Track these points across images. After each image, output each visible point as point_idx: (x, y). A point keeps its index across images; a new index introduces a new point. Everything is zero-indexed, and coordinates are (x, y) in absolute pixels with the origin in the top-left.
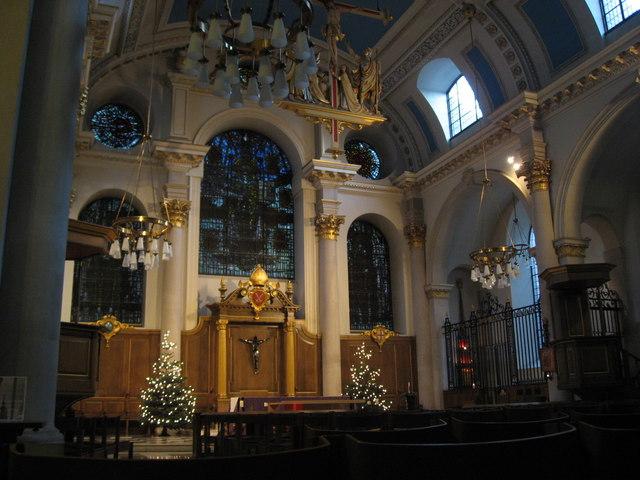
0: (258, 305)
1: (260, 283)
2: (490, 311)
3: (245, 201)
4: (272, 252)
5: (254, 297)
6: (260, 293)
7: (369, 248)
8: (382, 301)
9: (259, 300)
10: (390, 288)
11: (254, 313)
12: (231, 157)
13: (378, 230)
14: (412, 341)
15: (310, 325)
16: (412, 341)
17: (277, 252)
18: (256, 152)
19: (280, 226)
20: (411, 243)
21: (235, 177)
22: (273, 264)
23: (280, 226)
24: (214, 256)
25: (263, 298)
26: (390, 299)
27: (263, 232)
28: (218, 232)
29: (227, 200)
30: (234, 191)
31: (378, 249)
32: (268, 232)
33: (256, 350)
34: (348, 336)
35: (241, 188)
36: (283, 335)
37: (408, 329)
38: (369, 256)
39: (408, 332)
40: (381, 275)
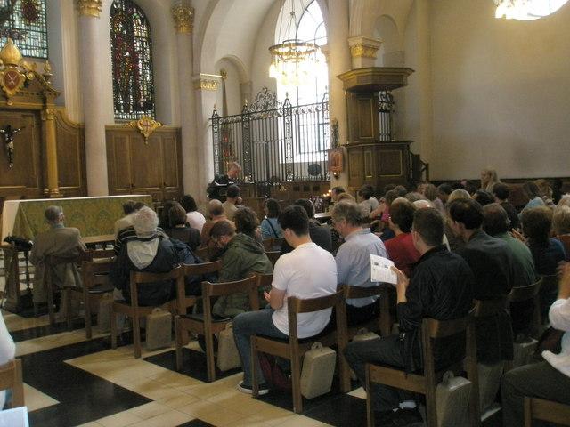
0: (11, 87)
1: (13, 62)
2: (265, 107)
4: (19, 23)
7: (129, 26)
8: (143, 89)
9: (12, 82)
10: (151, 75)
11: (6, 98)
13: (139, 8)
14: (178, 133)
15: (72, 115)
16: (178, 133)
17: (26, 25)
20: (177, 28)
22: (22, 39)
25: (17, 80)
26: (152, 90)
31: (140, 31)
33: (10, 141)
34: (113, 127)
36: (40, 125)
37: (173, 118)
38: (131, 39)
39: (173, 123)
40: (143, 60)
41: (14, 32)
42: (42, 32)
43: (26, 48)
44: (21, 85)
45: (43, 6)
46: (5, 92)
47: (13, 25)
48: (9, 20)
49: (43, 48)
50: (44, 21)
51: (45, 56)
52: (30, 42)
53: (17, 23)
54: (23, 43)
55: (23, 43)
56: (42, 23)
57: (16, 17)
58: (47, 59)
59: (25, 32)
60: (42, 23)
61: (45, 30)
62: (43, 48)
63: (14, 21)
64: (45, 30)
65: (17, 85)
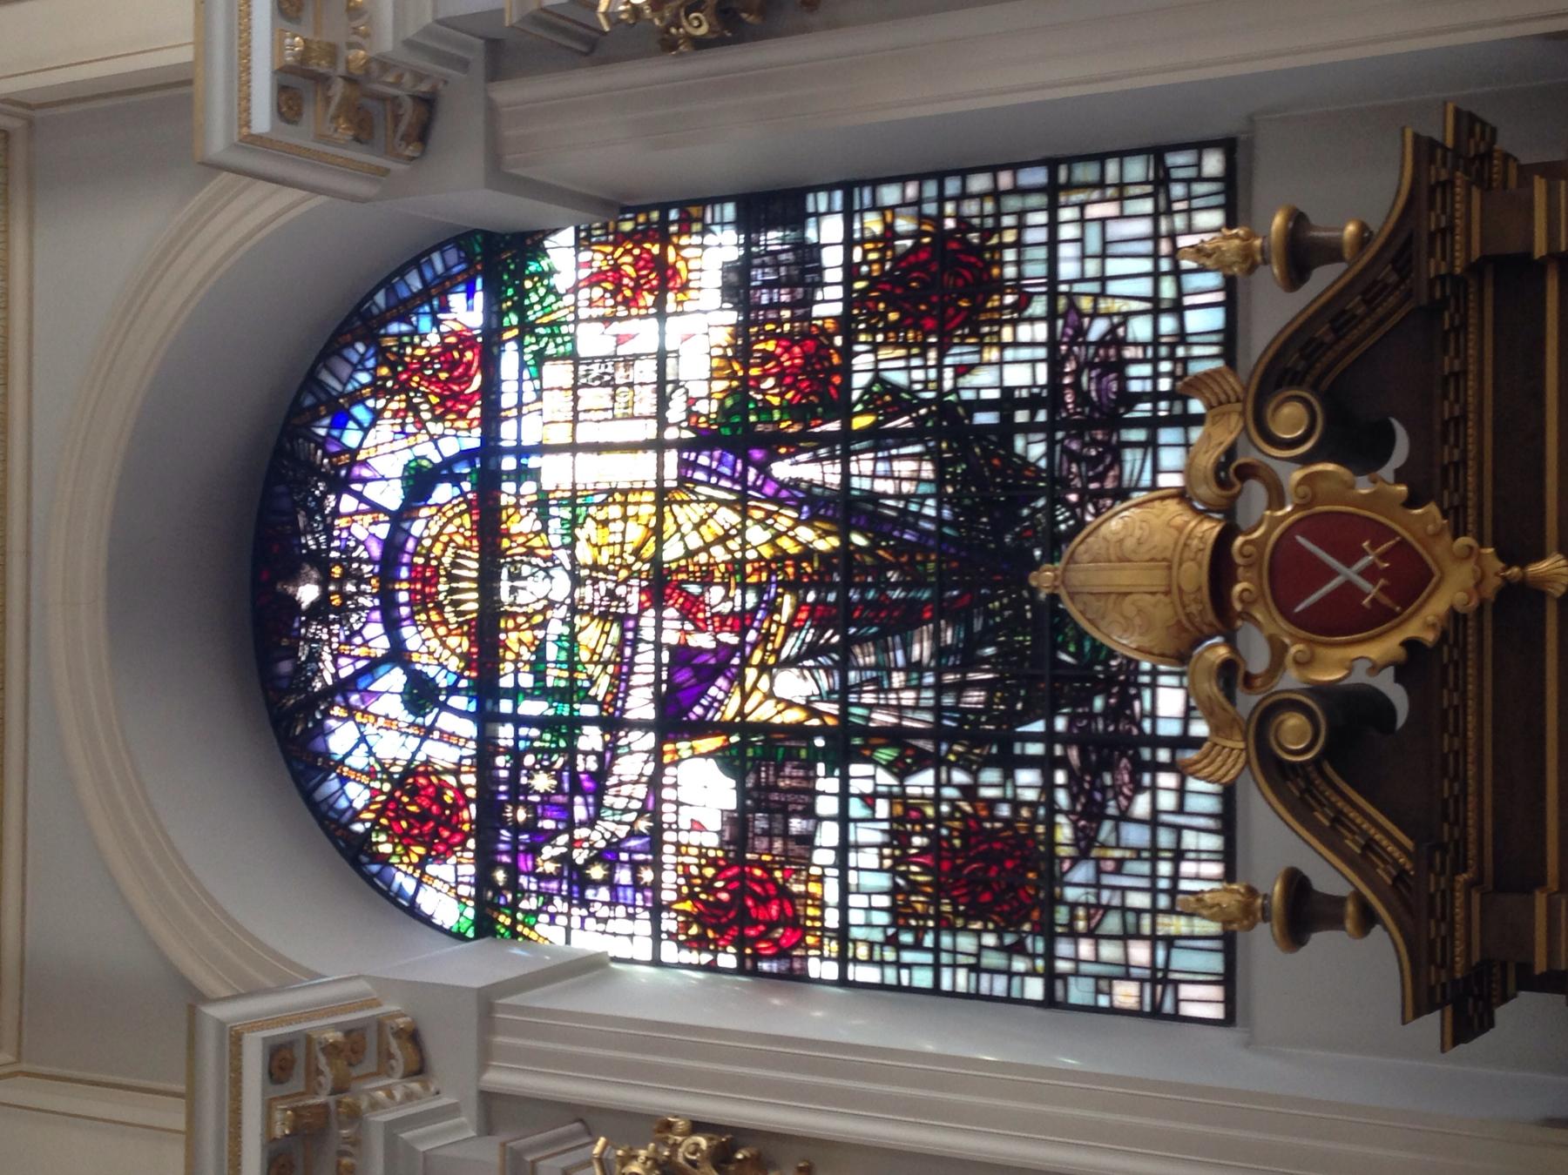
0: (1409, 578)
3: (661, 585)
4: (1015, 365)
5: (1343, 619)
6: (1288, 572)
11: (1516, 606)
12: (421, 695)
18: (375, 508)
19: (828, 305)
21: (538, 667)
23: (828, 305)
24: (1085, 844)
25: (1344, 532)
27: (879, 440)
28: (906, 815)
29: (676, 719)
30: (623, 674)
32: (886, 398)
35: (603, 616)
41: (1082, 397)
42: (1053, 193)
43: (1178, 308)
44: (1374, 489)
45: (890, 195)
46: (1455, 616)
47: (1033, 403)
48: (1007, 429)
49: (1161, 182)
50: (979, 183)
51: (1213, 163)
52: (1130, 278)
53: (1017, 376)
54: (1140, 329)
55: (1140, 329)
56: (996, 194)
57: (984, 383)
58: (1229, 147)
59: (1066, 315)
60: (996, 194)
61: (1038, 176)
62: (1161, 182)
63: (1008, 400)
64: (1038, 176)
65: (1380, 533)
